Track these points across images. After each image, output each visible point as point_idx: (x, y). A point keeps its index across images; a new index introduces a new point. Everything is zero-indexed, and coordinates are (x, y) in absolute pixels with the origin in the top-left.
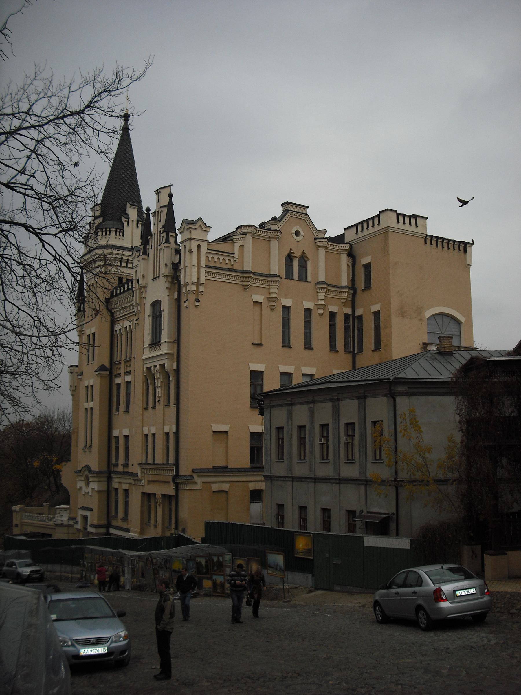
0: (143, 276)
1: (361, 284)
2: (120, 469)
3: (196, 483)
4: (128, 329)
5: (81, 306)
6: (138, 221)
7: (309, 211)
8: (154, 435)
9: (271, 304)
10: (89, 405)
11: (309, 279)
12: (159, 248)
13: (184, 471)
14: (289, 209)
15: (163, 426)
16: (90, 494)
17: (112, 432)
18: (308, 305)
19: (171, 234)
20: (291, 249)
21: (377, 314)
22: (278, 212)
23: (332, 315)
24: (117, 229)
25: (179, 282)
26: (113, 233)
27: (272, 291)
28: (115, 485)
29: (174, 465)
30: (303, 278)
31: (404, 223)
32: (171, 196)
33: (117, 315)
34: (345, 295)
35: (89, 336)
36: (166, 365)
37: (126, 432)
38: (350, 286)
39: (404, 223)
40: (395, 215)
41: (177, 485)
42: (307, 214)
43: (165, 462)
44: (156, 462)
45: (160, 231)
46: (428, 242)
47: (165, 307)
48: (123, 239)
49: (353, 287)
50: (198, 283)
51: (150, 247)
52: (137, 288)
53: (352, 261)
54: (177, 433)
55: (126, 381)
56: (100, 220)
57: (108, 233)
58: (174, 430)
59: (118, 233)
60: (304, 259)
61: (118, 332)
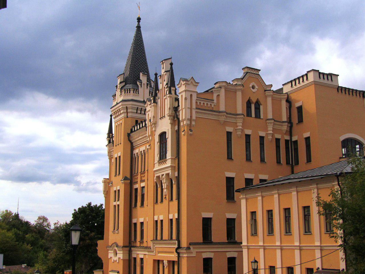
0: (154, 117)
1: (295, 120)
2: (138, 244)
3: (192, 253)
4: (142, 152)
5: (110, 139)
6: (147, 84)
7: (260, 73)
8: (162, 221)
9: (238, 133)
10: (116, 203)
11: (262, 117)
12: (165, 97)
13: (184, 243)
14: (248, 71)
15: (169, 214)
16: (117, 261)
17: (132, 220)
18: (262, 134)
19: (172, 88)
20: (250, 98)
21: (308, 139)
22: (241, 75)
23: (278, 141)
24: (134, 89)
25: (178, 119)
26: (132, 92)
27: (238, 124)
28: (134, 256)
29: (177, 240)
30: (258, 115)
31: (324, 78)
32: (171, 64)
33: (134, 144)
34: (285, 127)
35: (116, 158)
36: (170, 174)
37: (141, 220)
38: (288, 121)
39: (324, 78)
40: (318, 74)
41: (178, 254)
42: (259, 75)
43: (170, 238)
44: (163, 239)
45: (165, 87)
46: (340, 91)
47: (169, 136)
48: (138, 96)
49: (290, 121)
50: (191, 120)
51: (158, 98)
52: (149, 125)
53: (289, 105)
54: (178, 220)
55: (141, 186)
56: (123, 84)
57: (129, 92)
58: (176, 216)
59: (135, 92)
60: (258, 104)
61: (136, 155)
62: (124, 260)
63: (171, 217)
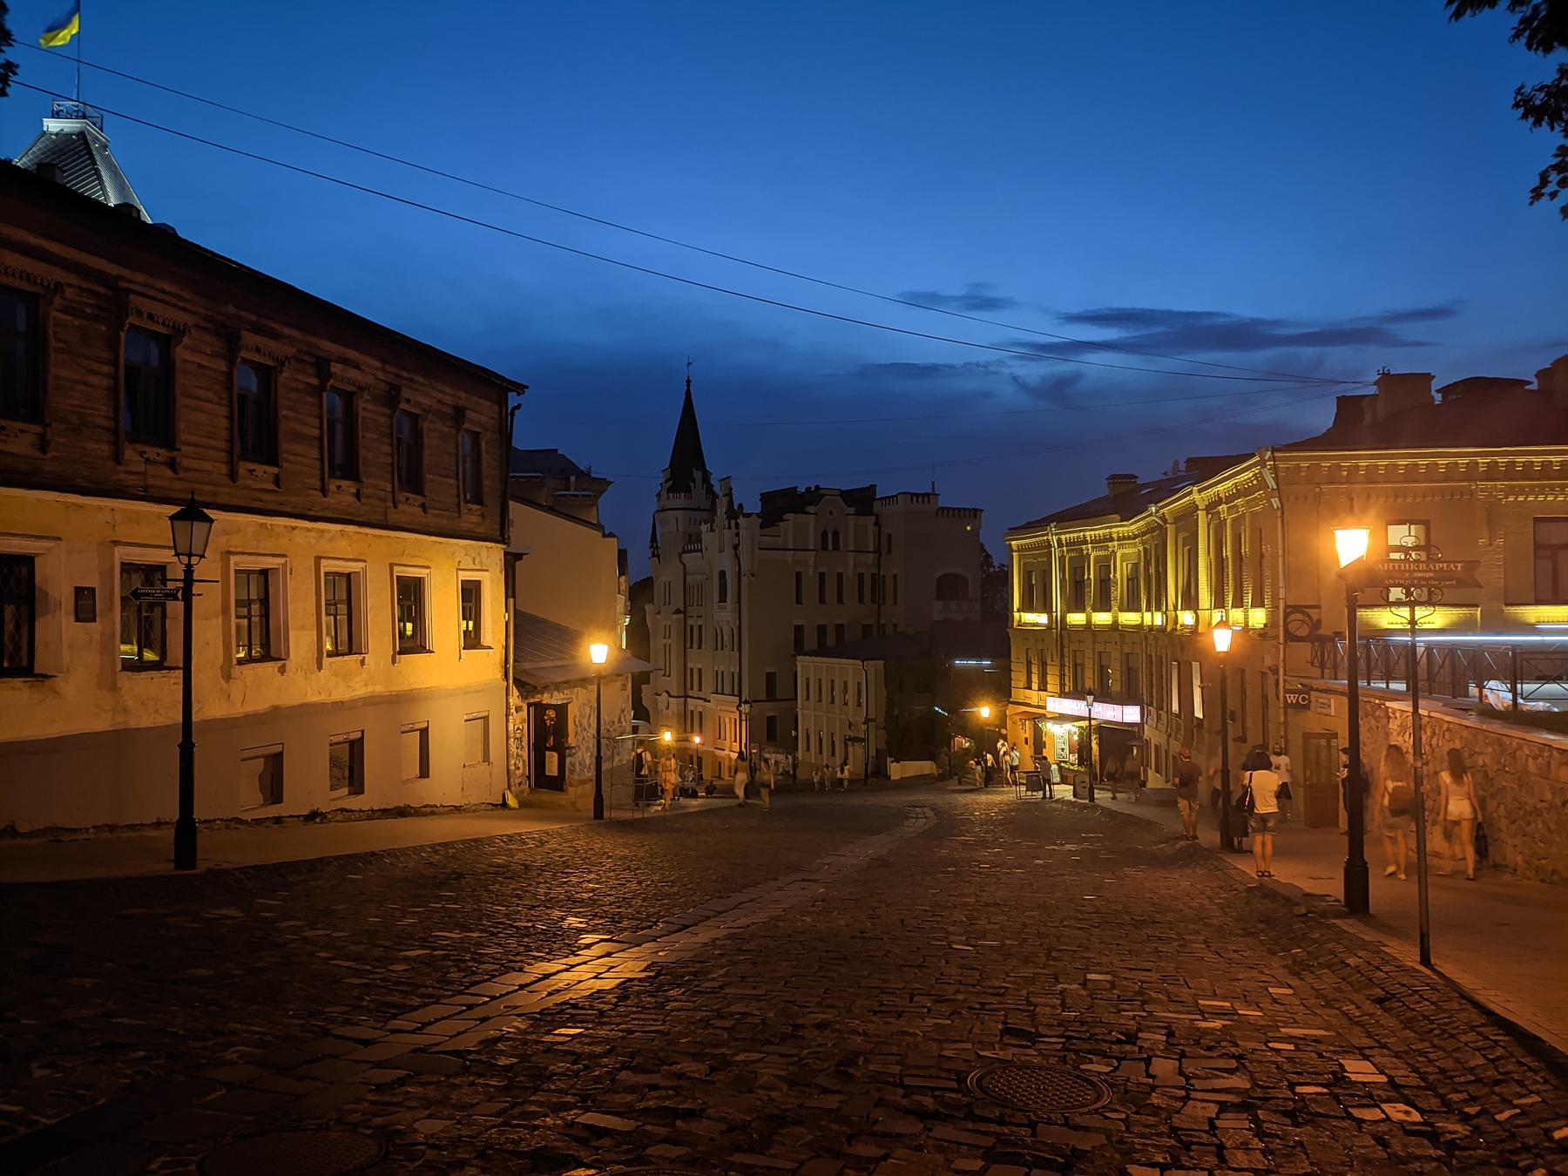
11: (841, 548)
18: (840, 570)
28: (691, 707)
30: (836, 548)
32: (731, 489)
34: (870, 558)
47: (728, 577)
49: (878, 551)
56: (670, 483)
62: (678, 715)
63: (732, 670)
